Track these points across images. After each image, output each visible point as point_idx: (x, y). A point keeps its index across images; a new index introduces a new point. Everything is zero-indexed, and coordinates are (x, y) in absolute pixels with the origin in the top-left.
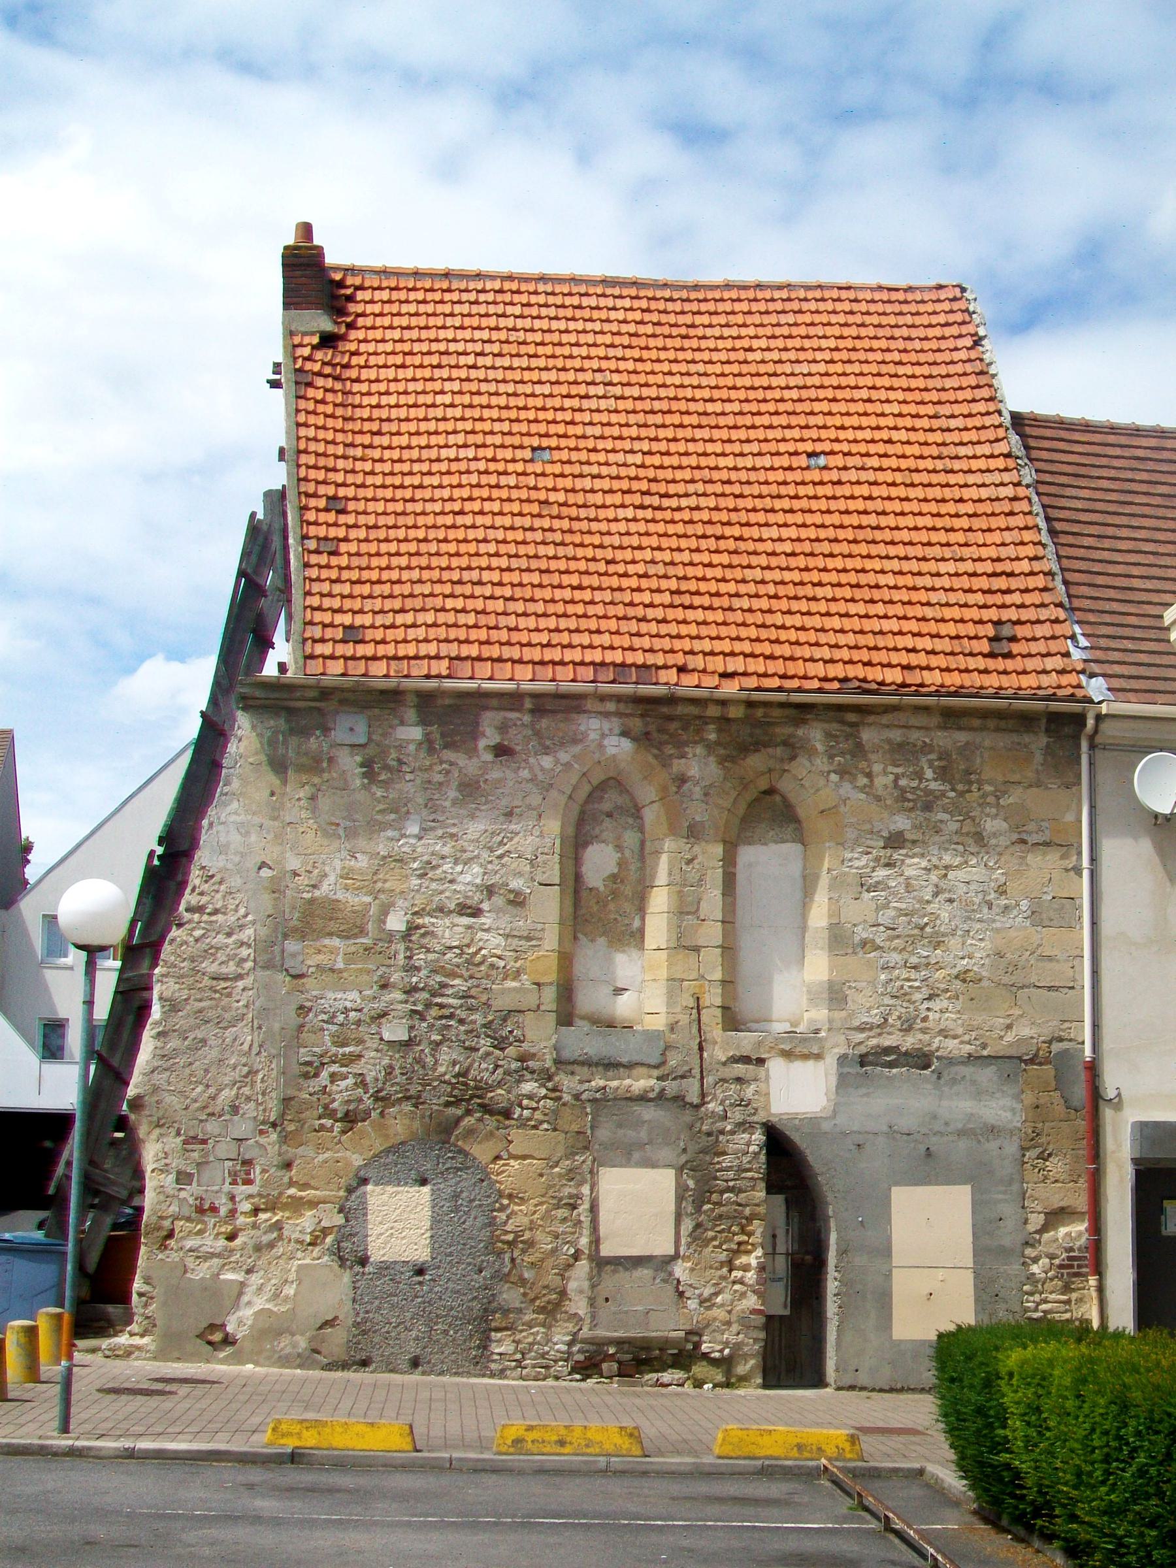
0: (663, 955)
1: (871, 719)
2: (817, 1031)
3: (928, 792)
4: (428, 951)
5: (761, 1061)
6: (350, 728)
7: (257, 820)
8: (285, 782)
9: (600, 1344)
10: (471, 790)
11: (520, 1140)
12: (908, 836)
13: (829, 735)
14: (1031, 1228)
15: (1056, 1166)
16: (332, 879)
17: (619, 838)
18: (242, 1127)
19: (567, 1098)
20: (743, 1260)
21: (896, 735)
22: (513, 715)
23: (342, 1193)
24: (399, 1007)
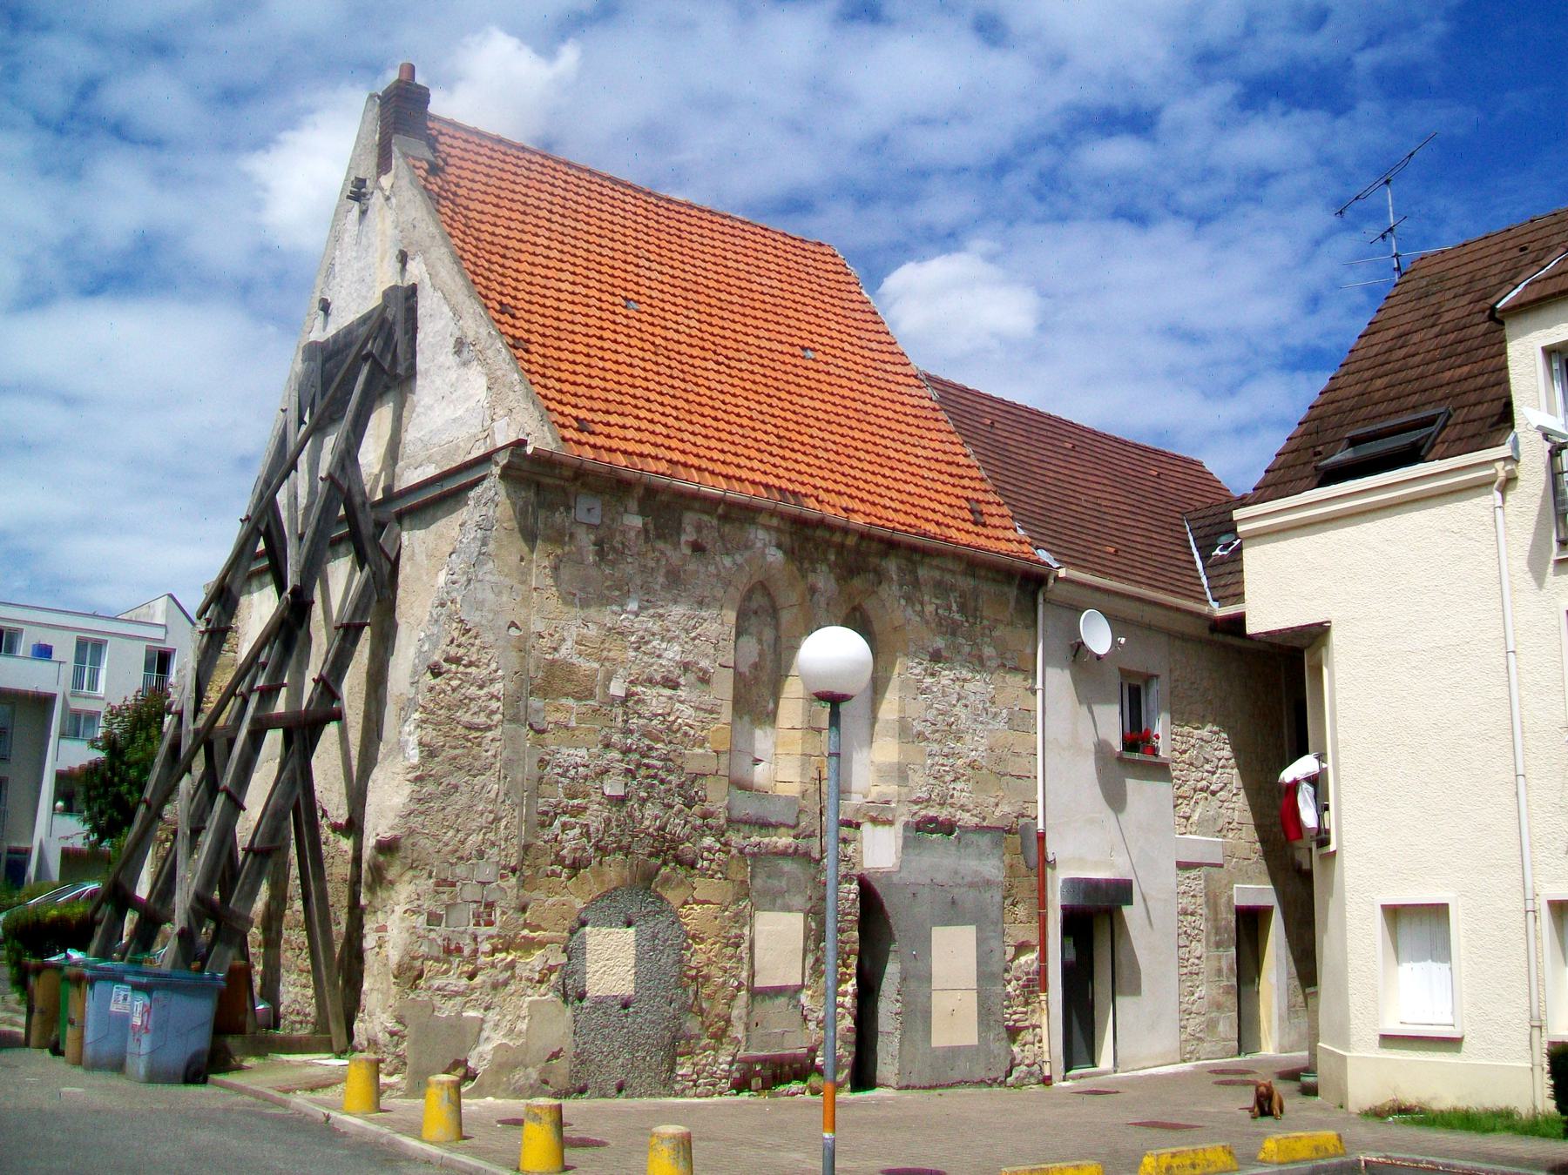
0: (799, 734)
1: (927, 560)
2: (887, 802)
3: (954, 621)
4: (640, 716)
5: (858, 826)
6: (588, 509)
7: (508, 582)
8: (532, 551)
9: (749, 1062)
10: (675, 580)
11: (703, 887)
12: (944, 654)
13: (899, 568)
14: (1008, 957)
15: (1021, 911)
16: (569, 643)
17: (760, 633)
18: (487, 871)
19: (734, 851)
20: (843, 987)
21: (937, 574)
22: (706, 518)
23: (566, 934)
24: (617, 765)
